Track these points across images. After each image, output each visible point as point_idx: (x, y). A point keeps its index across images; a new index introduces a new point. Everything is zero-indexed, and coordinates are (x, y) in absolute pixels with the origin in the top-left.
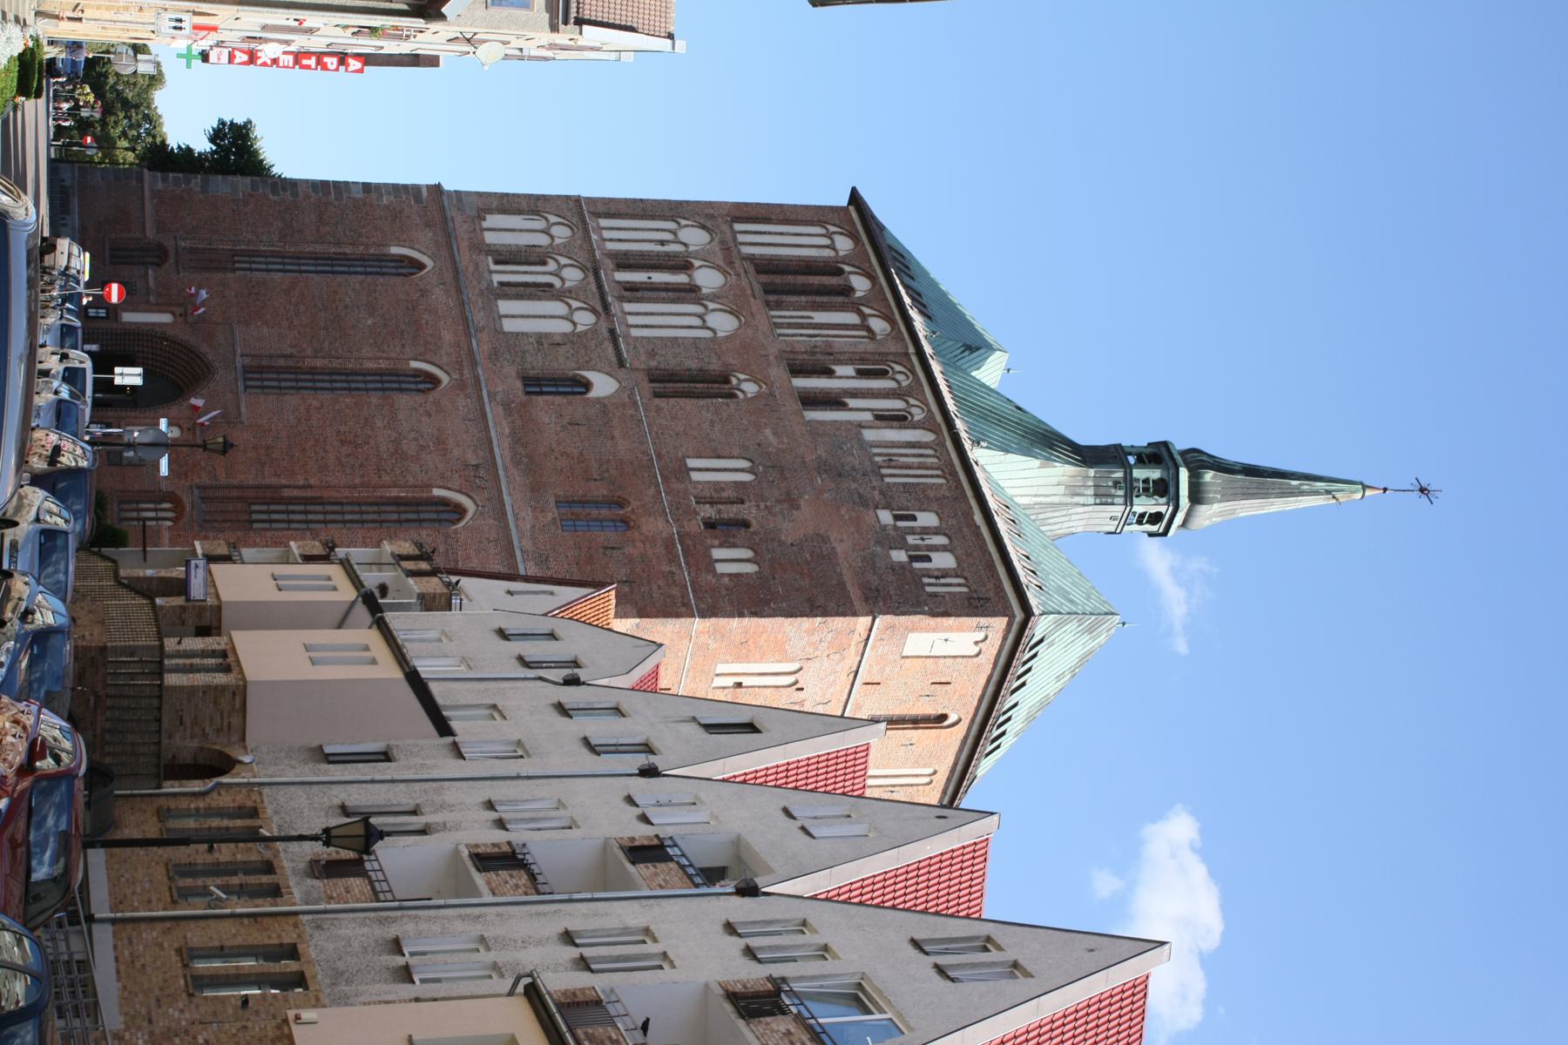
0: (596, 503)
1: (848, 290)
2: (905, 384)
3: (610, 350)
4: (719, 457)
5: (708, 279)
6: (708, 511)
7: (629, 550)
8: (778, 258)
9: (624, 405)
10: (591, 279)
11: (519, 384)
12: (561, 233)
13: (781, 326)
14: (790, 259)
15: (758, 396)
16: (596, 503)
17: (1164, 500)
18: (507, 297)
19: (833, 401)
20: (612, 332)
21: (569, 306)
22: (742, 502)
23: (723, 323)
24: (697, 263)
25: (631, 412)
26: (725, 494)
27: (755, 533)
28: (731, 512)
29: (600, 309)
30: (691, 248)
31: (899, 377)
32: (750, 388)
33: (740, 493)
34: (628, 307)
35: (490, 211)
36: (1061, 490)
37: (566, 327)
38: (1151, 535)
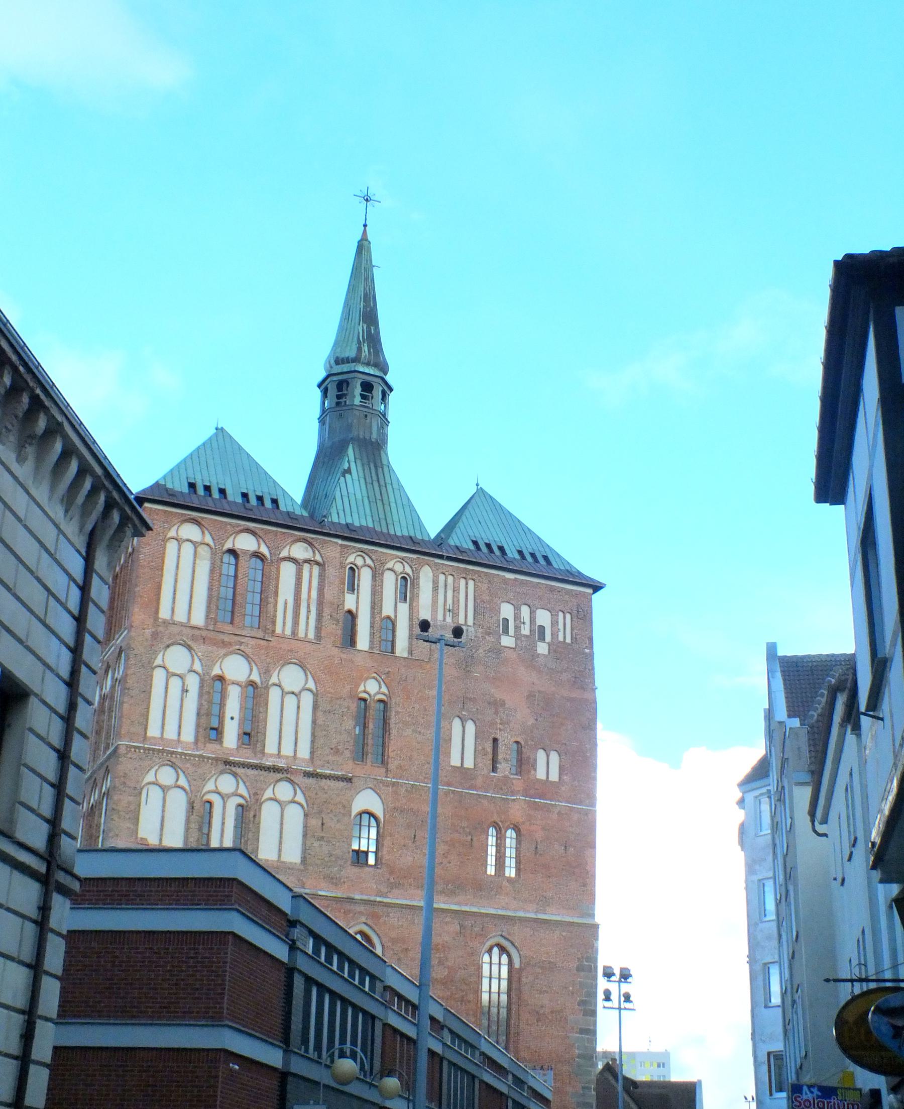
7: (539, 835)
9: (395, 793)
10: (240, 771)
20: (308, 775)
24: (216, 671)
25: (403, 790)
27: (526, 742)
29: (280, 776)
35: (136, 831)
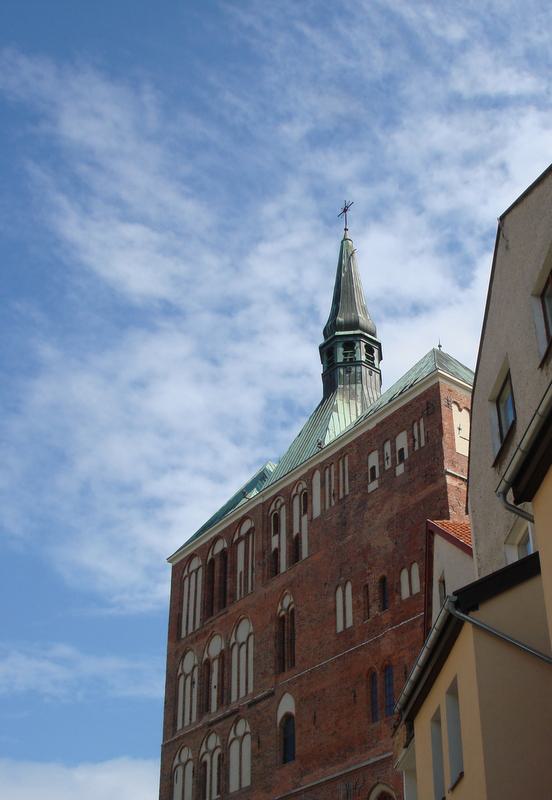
0: (373, 692)
1: (224, 553)
2: (283, 500)
3: (263, 704)
4: (335, 610)
5: (216, 646)
6: (375, 610)
8: (203, 602)
10: (215, 727)
11: (287, 766)
12: (186, 754)
13: (246, 590)
14: (204, 595)
15: (293, 594)
16: (373, 692)
17: (357, 345)
18: (227, 786)
19: (295, 544)
20: (250, 705)
21: (234, 739)
22: (367, 586)
23: (245, 629)
24: (206, 656)
26: (361, 599)
28: (374, 591)
29: (236, 716)
30: (196, 662)
31: (279, 504)
32: (287, 600)
33: (361, 589)
34: (234, 698)
36: (352, 402)
37: (248, 739)
38: (381, 358)
